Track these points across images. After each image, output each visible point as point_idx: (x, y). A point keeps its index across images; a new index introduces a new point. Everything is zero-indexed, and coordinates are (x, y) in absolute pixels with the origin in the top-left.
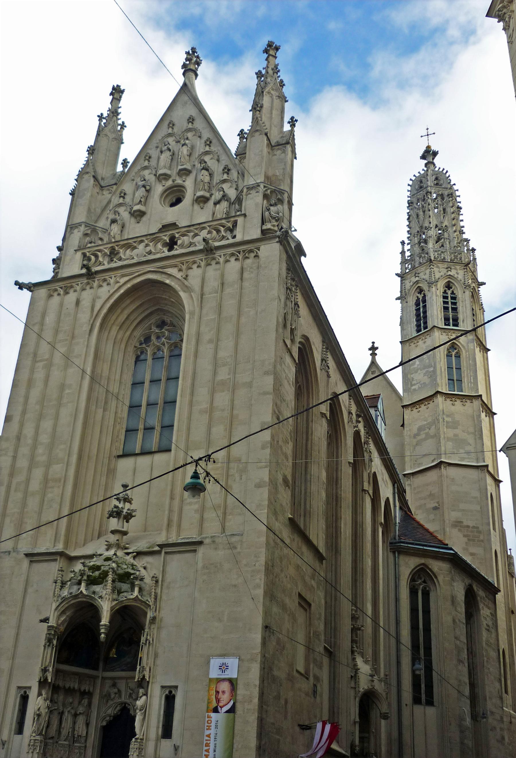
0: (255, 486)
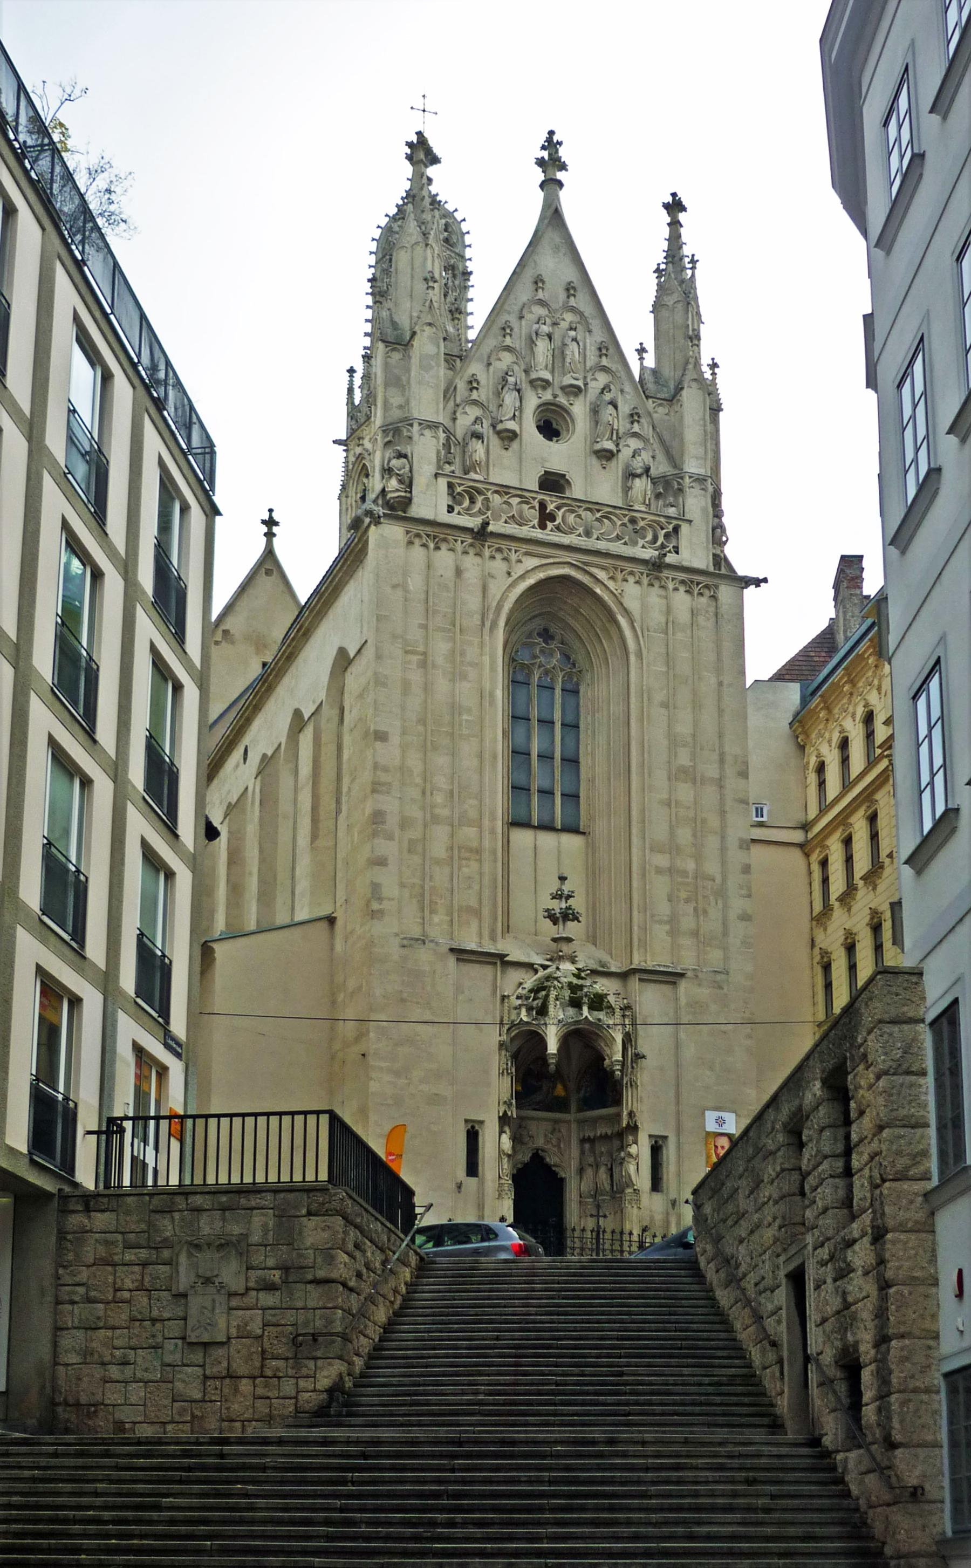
0: (738, 918)
